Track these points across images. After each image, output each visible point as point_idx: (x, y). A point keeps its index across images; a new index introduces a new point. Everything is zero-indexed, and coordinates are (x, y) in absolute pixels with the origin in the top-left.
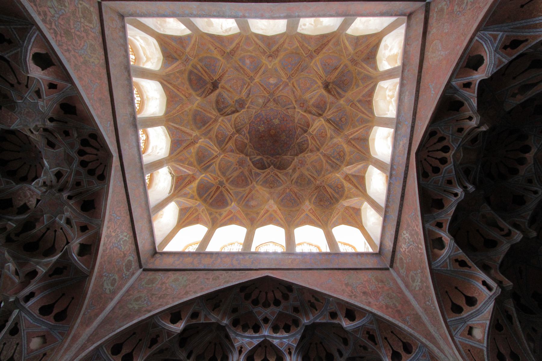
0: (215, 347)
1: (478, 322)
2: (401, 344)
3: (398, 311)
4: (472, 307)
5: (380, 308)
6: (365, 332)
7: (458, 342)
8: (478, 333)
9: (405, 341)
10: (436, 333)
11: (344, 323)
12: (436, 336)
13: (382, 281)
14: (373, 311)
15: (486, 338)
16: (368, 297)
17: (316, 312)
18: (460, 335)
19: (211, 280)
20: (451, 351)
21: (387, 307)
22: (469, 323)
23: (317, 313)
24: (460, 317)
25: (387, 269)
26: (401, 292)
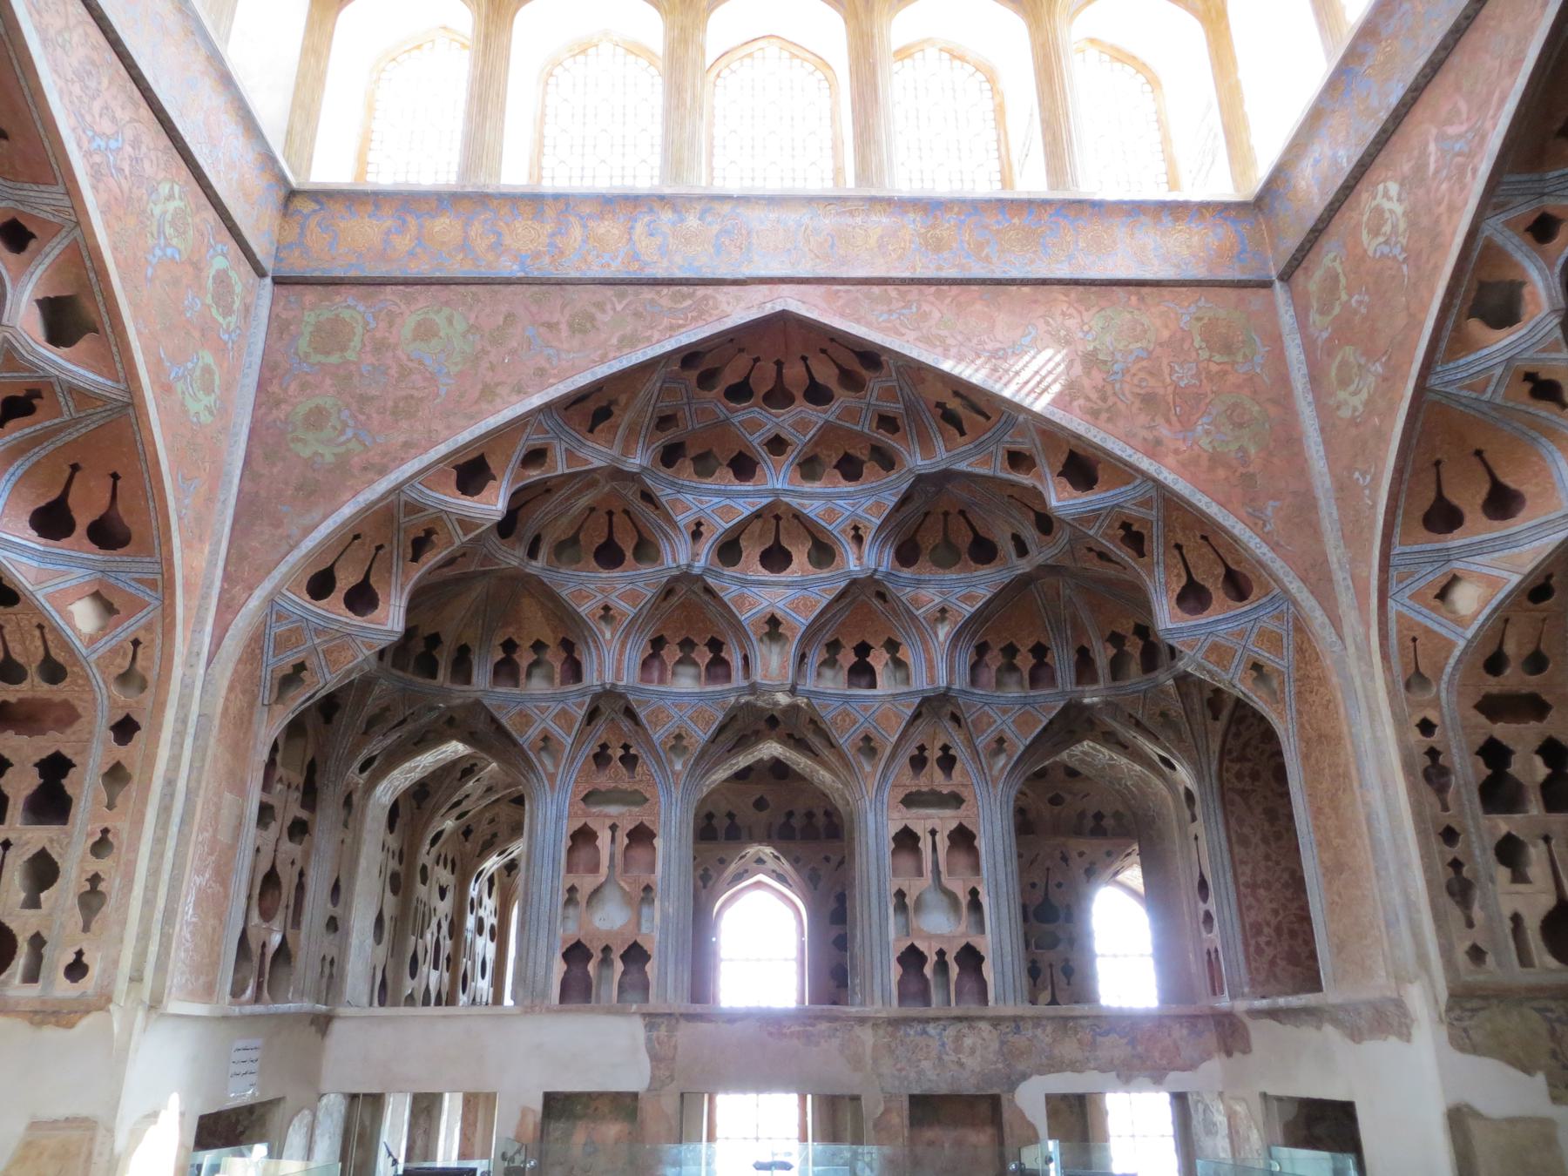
0: (610, 521)
1: (1485, 570)
2: (1221, 571)
3: (1248, 479)
4: (1496, 523)
5: (1187, 466)
6: (1117, 525)
7: (1392, 615)
8: (1467, 599)
9: (1234, 567)
10: (1341, 567)
11: (1053, 495)
12: (1340, 576)
13: (1228, 348)
14: (1161, 478)
15: (1481, 618)
16: (1160, 420)
17: (960, 440)
18: (1410, 597)
19: (564, 331)
20: (1361, 630)
21: (1216, 460)
22: (1457, 565)
23: (963, 445)
24: (1438, 546)
25: (1266, 284)
26: (1283, 398)
